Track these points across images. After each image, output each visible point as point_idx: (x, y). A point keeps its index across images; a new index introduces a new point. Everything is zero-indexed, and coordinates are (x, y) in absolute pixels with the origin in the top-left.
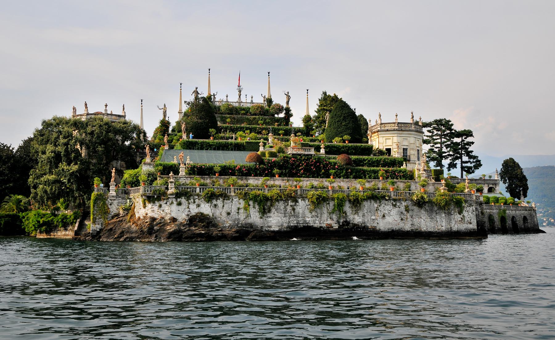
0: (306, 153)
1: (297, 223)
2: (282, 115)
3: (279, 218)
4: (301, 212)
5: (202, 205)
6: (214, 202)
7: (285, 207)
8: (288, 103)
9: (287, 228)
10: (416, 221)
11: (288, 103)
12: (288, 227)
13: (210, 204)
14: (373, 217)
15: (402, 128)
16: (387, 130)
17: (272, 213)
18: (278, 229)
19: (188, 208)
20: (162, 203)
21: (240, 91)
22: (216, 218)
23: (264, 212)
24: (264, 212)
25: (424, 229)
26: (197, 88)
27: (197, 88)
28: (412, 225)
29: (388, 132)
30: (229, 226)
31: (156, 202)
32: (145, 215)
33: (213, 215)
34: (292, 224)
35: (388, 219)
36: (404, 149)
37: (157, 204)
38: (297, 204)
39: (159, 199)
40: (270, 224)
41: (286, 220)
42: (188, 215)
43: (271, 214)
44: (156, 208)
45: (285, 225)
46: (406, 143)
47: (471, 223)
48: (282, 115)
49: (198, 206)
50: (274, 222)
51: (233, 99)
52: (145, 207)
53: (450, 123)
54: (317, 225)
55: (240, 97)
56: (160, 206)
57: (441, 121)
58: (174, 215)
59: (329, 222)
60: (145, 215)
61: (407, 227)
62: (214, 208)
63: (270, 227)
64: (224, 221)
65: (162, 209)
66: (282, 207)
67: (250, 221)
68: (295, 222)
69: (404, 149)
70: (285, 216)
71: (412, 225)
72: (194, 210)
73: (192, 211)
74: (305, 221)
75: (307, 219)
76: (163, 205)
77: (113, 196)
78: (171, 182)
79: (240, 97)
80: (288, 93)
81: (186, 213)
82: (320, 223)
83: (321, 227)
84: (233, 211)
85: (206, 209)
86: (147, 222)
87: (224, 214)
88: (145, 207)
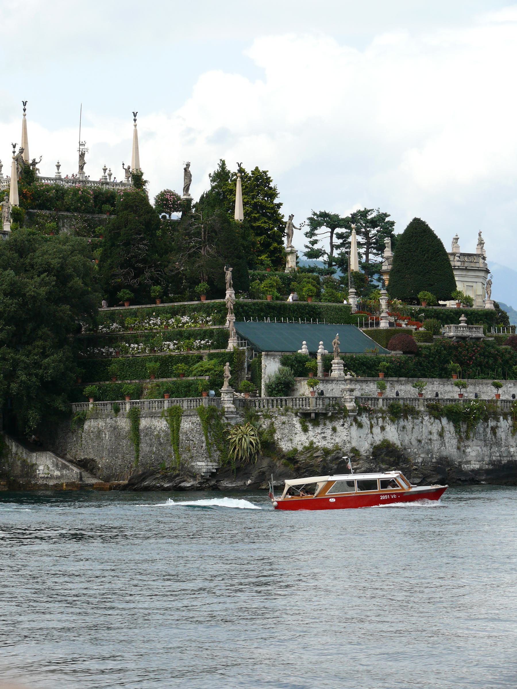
1: (500, 456)
3: (478, 448)
4: (503, 437)
5: (388, 428)
6: (402, 423)
7: (484, 429)
8: (186, 189)
9: (488, 464)
12: (491, 463)
13: (396, 426)
17: (471, 440)
18: (478, 467)
19: (371, 433)
20: (338, 424)
22: (405, 449)
23: (463, 438)
24: (463, 438)
30: (422, 463)
31: (328, 422)
32: (307, 445)
33: (402, 445)
34: (494, 458)
37: (330, 426)
38: (499, 424)
39: (332, 418)
40: (469, 458)
41: (486, 450)
42: (372, 445)
43: (469, 443)
44: (329, 432)
45: (487, 459)
49: (383, 429)
50: (473, 454)
52: (305, 430)
53: (387, 219)
55: (81, 168)
56: (334, 430)
57: (364, 214)
58: (354, 444)
60: (307, 445)
62: (402, 433)
63: (468, 462)
64: (416, 454)
65: (337, 434)
66: (481, 430)
67: (444, 454)
68: (498, 454)
70: (486, 445)
72: (378, 437)
73: (376, 438)
74: (509, 452)
75: (512, 450)
76: (339, 428)
77: (232, 412)
80: (188, 165)
81: (369, 442)
84: (424, 437)
85: (392, 434)
86: (317, 457)
87: (415, 443)
88: (305, 430)
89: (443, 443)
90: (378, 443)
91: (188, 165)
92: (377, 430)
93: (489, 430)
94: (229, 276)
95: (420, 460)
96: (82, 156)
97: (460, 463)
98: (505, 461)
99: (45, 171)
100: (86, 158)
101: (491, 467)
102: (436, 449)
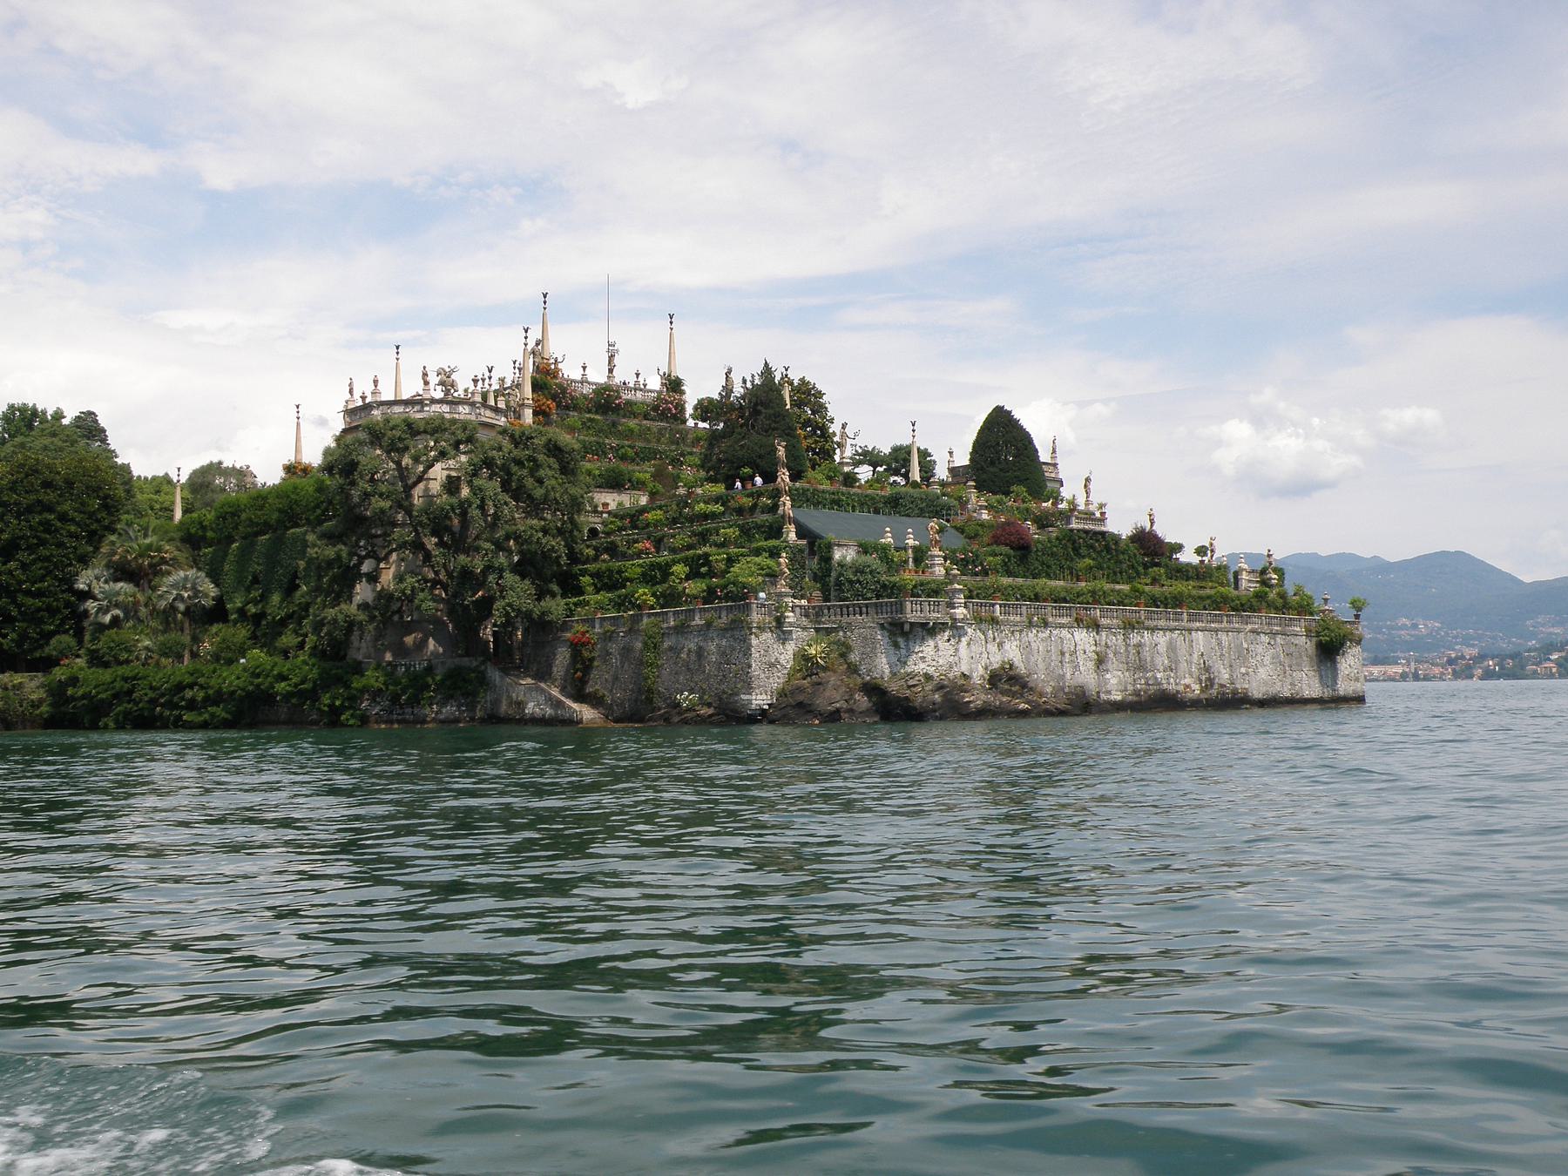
5: (1007, 646)
12: (1136, 693)
14: (1243, 670)
18: (1119, 698)
21: (611, 358)
25: (1307, 694)
35: (1263, 673)
45: (1130, 688)
49: (1000, 645)
50: (1114, 681)
51: (598, 376)
54: (1171, 687)
55: (611, 371)
58: (964, 668)
59: (1187, 681)
63: (1109, 692)
72: (996, 661)
77: (791, 624)
79: (611, 371)
89: (1076, 667)
90: (996, 666)
91: (730, 371)
92: (993, 648)
94: (781, 452)
95: (1049, 690)
96: (611, 358)
99: (570, 371)
100: (616, 360)
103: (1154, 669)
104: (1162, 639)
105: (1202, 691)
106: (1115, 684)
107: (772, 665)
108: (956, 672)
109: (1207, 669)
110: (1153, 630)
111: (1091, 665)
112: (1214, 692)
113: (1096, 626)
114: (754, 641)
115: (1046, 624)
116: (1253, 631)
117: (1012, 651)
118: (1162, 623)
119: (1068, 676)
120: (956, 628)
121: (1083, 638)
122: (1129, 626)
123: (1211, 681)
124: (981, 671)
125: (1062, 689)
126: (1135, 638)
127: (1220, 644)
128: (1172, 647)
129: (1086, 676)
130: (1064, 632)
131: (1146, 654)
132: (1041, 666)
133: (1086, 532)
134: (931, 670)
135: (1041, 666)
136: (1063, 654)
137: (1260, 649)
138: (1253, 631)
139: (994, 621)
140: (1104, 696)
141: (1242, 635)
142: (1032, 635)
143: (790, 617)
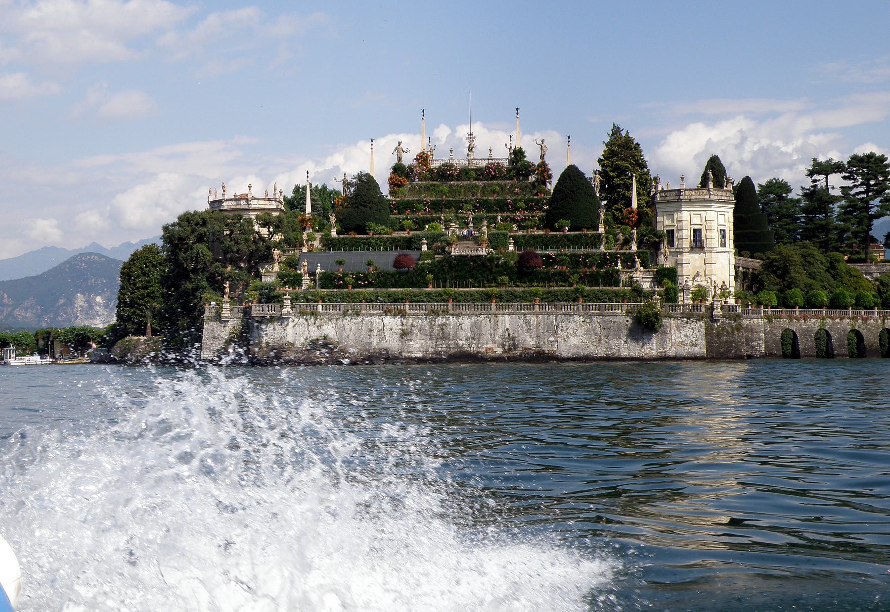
0: (474, 253)
2: (532, 178)
5: (325, 327)
7: (431, 328)
10: (614, 342)
11: (542, 157)
14: (552, 339)
15: (692, 197)
16: (668, 202)
25: (625, 354)
26: (400, 144)
27: (400, 144)
28: (606, 348)
29: (669, 205)
36: (695, 230)
46: (696, 220)
47: (696, 345)
48: (532, 178)
49: (319, 327)
50: (417, 346)
54: (473, 348)
58: (290, 339)
61: (601, 352)
63: (412, 352)
67: (384, 345)
69: (695, 230)
71: (606, 348)
74: (458, 344)
75: (461, 343)
78: (287, 299)
82: (478, 347)
83: (478, 352)
90: (314, 338)
93: (436, 328)
97: (400, 353)
98: (452, 351)
101: (434, 356)
102: (375, 343)
103: (456, 337)
104: (467, 322)
105: (504, 351)
106: (417, 347)
107: (215, 338)
108: (284, 341)
109: (513, 339)
110: (458, 316)
111: (397, 337)
112: (517, 352)
113: (403, 314)
114: (205, 326)
115: (358, 315)
116: (565, 314)
117: (329, 330)
118: (463, 312)
119: (375, 343)
120: (281, 319)
121: (392, 323)
122: (435, 313)
123: (515, 346)
124: (302, 340)
125: (368, 351)
126: (440, 320)
127: (528, 323)
128: (476, 326)
129: (392, 343)
130: (375, 319)
131: (450, 330)
132: (351, 337)
133: (466, 256)
134: (270, 341)
135: (351, 337)
136: (371, 331)
137: (573, 325)
138: (565, 314)
139: (314, 314)
140: (405, 354)
141: (553, 318)
142: (346, 321)
143: (226, 313)
